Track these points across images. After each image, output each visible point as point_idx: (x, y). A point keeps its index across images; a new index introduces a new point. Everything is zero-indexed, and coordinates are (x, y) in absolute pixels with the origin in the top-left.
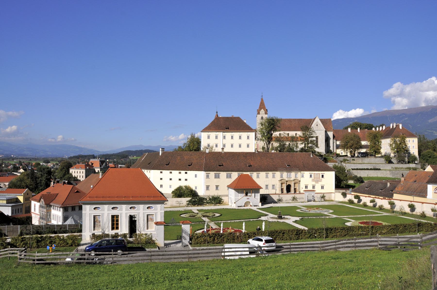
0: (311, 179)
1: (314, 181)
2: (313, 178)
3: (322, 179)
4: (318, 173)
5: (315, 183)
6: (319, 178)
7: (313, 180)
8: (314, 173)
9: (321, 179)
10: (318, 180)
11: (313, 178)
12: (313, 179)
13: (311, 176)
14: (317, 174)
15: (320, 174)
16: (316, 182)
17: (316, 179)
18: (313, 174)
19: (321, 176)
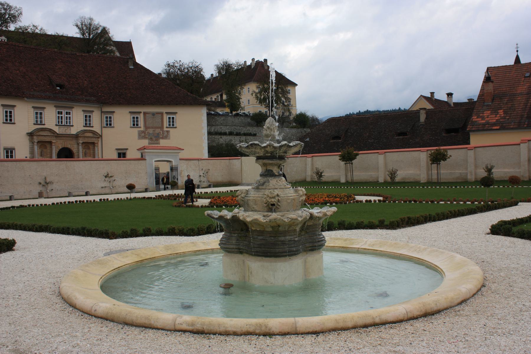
0: (136, 131)
1: (144, 138)
2: (142, 129)
3: (172, 131)
4: (158, 113)
5: (149, 143)
6: (162, 127)
7: (142, 135)
8: (145, 113)
9: (165, 129)
10: (158, 134)
11: (142, 129)
12: (143, 132)
13: (135, 124)
14: (153, 114)
15: (162, 114)
16: (151, 139)
17: (151, 131)
18: (142, 115)
19: (166, 123)
